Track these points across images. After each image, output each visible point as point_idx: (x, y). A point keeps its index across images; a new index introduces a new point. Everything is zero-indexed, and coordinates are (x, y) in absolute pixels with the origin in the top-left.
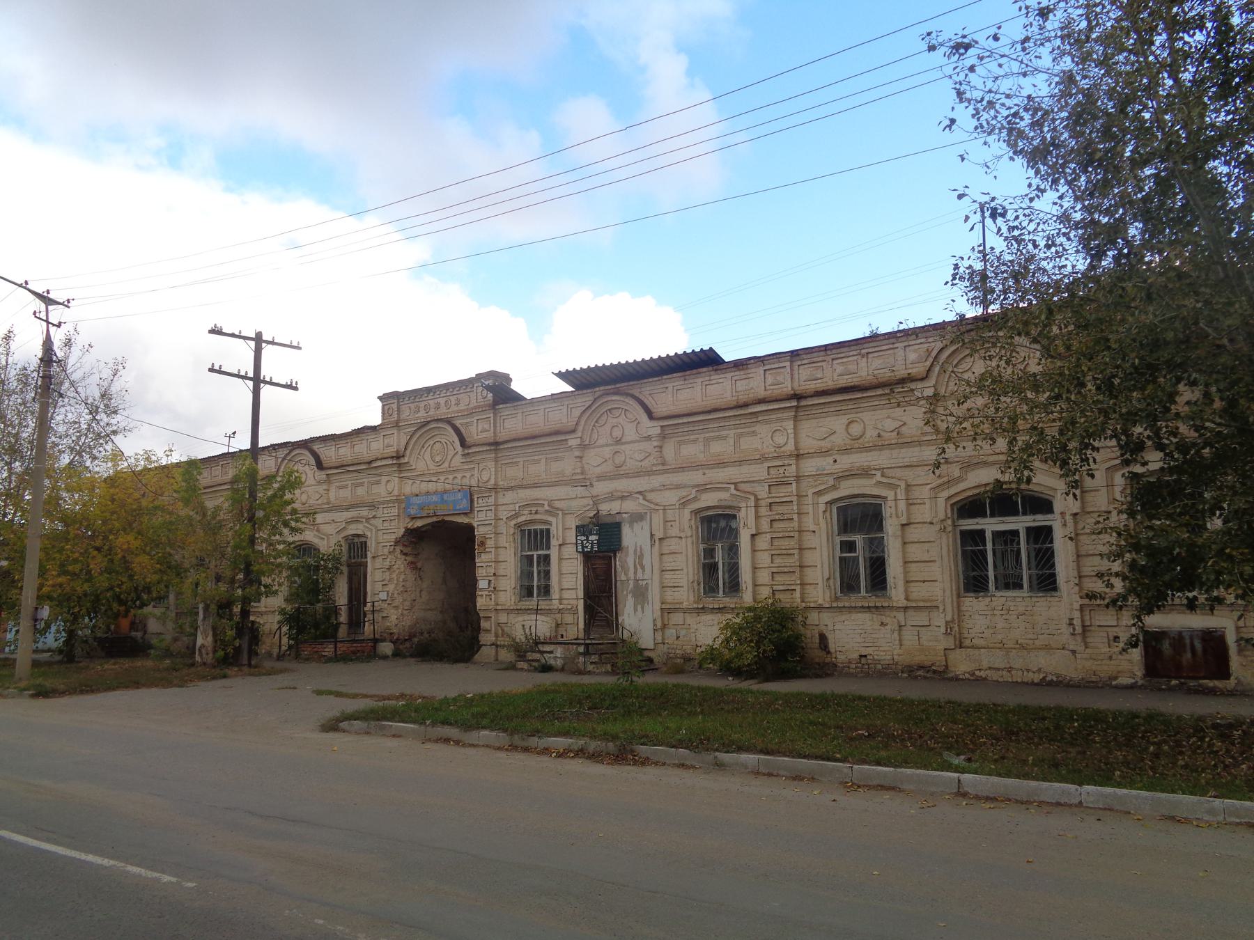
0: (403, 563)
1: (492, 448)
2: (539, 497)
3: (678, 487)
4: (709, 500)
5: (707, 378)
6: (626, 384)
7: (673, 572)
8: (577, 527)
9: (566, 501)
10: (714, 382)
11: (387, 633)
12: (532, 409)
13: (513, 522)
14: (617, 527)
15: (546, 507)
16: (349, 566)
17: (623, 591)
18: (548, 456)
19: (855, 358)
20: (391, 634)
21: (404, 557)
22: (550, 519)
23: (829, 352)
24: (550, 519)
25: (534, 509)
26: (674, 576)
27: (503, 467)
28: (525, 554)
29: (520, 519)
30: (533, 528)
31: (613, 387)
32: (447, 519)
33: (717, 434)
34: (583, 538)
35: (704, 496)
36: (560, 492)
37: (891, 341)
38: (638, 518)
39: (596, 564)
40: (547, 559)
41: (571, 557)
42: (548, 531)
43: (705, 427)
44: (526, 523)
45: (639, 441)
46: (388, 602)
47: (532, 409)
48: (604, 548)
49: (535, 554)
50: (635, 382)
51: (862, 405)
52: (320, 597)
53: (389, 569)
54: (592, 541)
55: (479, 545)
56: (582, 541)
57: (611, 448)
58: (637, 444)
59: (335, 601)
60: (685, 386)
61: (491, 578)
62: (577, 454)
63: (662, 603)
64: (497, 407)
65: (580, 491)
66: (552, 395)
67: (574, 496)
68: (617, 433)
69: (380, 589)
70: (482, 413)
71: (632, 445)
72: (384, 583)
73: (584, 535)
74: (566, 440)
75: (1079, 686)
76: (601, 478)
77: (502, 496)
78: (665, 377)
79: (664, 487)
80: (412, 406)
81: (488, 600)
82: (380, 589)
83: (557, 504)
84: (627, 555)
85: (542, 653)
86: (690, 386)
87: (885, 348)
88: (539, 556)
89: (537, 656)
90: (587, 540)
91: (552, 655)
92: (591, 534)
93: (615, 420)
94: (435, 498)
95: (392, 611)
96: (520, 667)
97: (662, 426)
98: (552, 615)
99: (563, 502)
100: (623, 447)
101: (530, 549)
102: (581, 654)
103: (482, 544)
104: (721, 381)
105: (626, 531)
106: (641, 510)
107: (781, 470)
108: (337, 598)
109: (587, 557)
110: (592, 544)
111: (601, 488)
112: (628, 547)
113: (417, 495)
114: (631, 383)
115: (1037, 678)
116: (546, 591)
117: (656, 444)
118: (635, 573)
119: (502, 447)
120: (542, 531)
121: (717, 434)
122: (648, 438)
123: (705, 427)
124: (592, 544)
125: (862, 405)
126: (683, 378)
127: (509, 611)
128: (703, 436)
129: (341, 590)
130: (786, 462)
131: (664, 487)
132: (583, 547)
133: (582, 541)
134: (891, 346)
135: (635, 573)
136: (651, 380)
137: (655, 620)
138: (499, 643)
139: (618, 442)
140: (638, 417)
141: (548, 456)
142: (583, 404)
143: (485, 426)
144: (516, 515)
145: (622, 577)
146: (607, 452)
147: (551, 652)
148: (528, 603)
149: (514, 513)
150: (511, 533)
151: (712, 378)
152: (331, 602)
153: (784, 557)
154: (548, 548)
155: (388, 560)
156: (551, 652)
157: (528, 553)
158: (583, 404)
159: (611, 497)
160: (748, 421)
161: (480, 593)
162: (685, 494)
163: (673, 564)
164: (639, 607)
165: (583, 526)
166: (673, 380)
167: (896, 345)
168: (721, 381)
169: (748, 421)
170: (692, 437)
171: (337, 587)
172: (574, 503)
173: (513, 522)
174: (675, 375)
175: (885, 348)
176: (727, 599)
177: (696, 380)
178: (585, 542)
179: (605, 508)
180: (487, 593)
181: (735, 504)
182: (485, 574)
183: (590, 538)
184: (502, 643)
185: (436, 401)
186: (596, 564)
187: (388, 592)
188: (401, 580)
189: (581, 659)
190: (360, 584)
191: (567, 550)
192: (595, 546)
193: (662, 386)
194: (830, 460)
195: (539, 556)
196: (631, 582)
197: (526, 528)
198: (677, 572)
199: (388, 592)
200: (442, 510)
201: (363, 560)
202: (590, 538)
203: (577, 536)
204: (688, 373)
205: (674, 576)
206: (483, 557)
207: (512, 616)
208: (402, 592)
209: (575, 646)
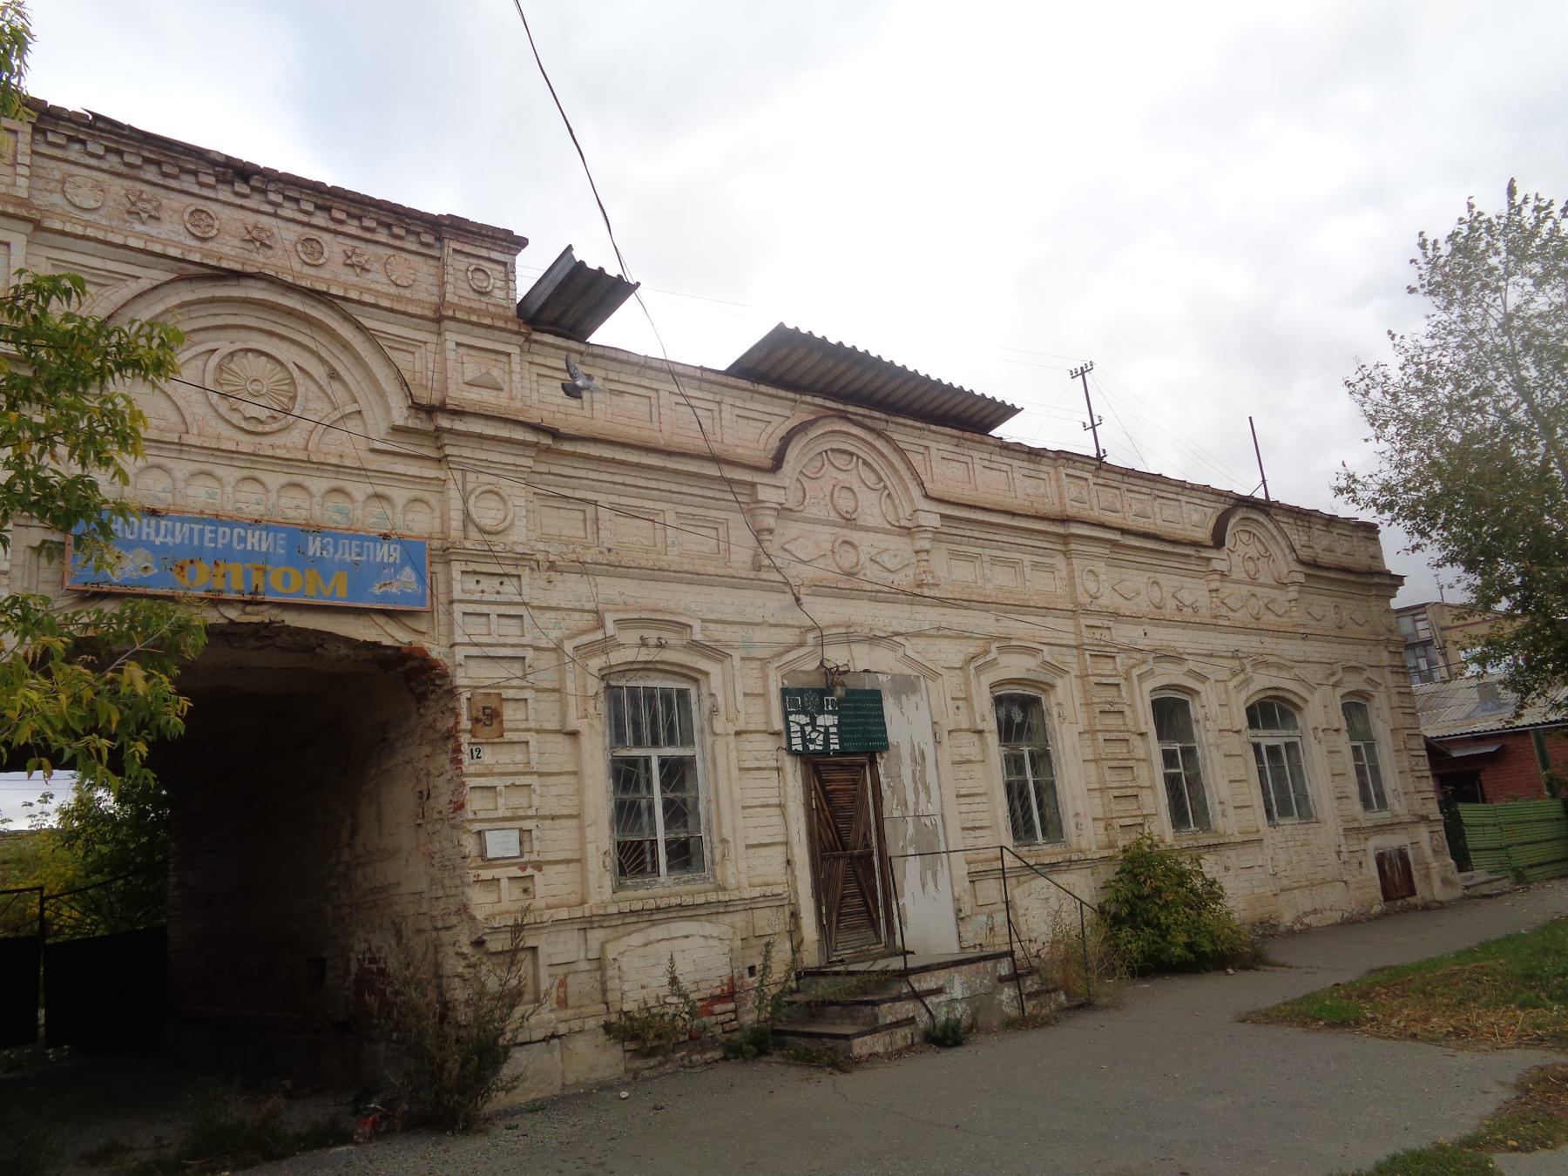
1: (546, 441)
2: (662, 605)
3: (961, 635)
4: (1015, 666)
5: (987, 456)
6: (866, 412)
7: (968, 800)
8: (785, 692)
9: (735, 628)
10: (994, 465)
12: (635, 380)
13: (595, 663)
14: (875, 697)
15: (698, 636)
17: (897, 844)
18: (681, 509)
19: (1146, 497)
22: (703, 664)
23: (1126, 479)
24: (703, 664)
25: (652, 636)
26: (975, 808)
27: (537, 503)
28: (624, 753)
29: (617, 657)
30: (641, 684)
31: (841, 407)
32: (293, 620)
33: (1006, 554)
34: (804, 719)
35: (1005, 660)
36: (725, 602)
37: (1179, 490)
38: (906, 686)
39: (830, 781)
40: (677, 772)
41: (763, 764)
42: (682, 694)
43: (997, 537)
44: (631, 668)
45: (886, 532)
47: (635, 380)
48: (851, 746)
49: (654, 755)
50: (883, 416)
51: (1165, 563)
54: (827, 728)
55: (476, 720)
56: (802, 726)
57: (836, 530)
58: (881, 536)
60: (955, 457)
61: (527, 825)
62: (769, 521)
63: (968, 863)
64: (536, 336)
65: (771, 605)
66: (702, 369)
67: (759, 620)
68: (845, 502)
70: (483, 332)
71: (872, 535)
73: (804, 712)
74: (753, 485)
75: (1359, 921)
76: (822, 589)
77: (543, 583)
78: (933, 427)
79: (939, 633)
80: (117, 186)
81: (517, 893)
83: (717, 632)
84: (899, 764)
85: (918, 996)
86: (962, 458)
87: (1170, 496)
88: (664, 762)
89: (907, 1009)
90: (813, 723)
91: (943, 998)
92: (821, 712)
93: (841, 476)
94: (256, 541)
96: (865, 1051)
97: (943, 516)
98: (727, 918)
99: (728, 627)
100: (855, 536)
101: (638, 742)
102: (1002, 979)
103: (489, 716)
104: (1004, 468)
105: (889, 708)
106: (907, 671)
107: (1098, 633)
109: (814, 764)
110: (827, 734)
111: (825, 611)
112: (898, 745)
113: (153, 513)
114: (876, 414)
115: (1337, 917)
116: (684, 855)
117: (927, 545)
118: (917, 803)
119: (568, 447)
120: (666, 696)
121: (1006, 554)
122: (908, 532)
123: (997, 537)
124: (827, 734)
125: (1165, 563)
126: (954, 441)
127: (587, 924)
128: (987, 551)
130: (1106, 623)
131: (939, 633)
132: (806, 740)
133: (802, 726)
134: (1175, 496)
135: (917, 803)
136: (910, 422)
137: (956, 900)
138: (562, 1029)
139: (849, 521)
140: (889, 484)
141: (681, 509)
142: (766, 418)
143: (495, 373)
144: (606, 645)
145: (891, 807)
146: (825, 535)
147: (938, 991)
148: (641, 893)
149: (599, 635)
150: (591, 692)
151: (994, 458)
153: (1120, 771)
154: (688, 741)
156: (938, 991)
157: (636, 752)
158: (766, 418)
159: (849, 638)
160: (1050, 546)
161: (486, 874)
162: (972, 650)
163: (968, 783)
164: (929, 874)
165: (801, 692)
166: (939, 437)
167: (1180, 497)
168: (1004, 468)
169: (1050, 546)
170: (972, 550)
172: (759, 635)
173: (595, 663)
174: (948, 430)
175: (1170, 496)
176: (1048, 846)
177: (972, 453)
178: (808, 729)
179: (837, 656)
180: (517, 872)
181: (1048, 679)
182: (501, 813)
183: (821, 720)
184: (576, 1025)
185: (251, 218)
186: (830, 781)
189: (1008, 992)
191: (749, 747)
192: (834, 740)
193: (919, 441)
194: (1140, 630)
195: (664, 762)
196: (911, 830)
197: (622, 683)
198: (977, 799)
200: (278, 586)
202: (821, 720)
203: (786, 715)
204: (968, 435)
205: (975, 808)
206: (488, 755)
207: (596, 936)
209: (989, 964)
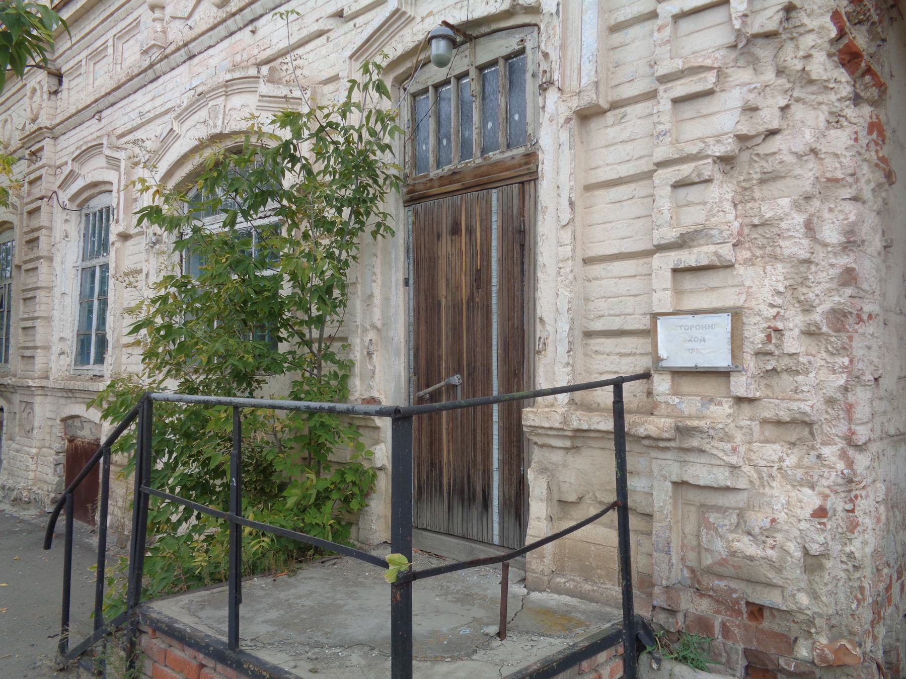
0: (836, 120)
11: (723, 602)
16: (413, 199)
20: (757, 611)
21: (842, 75)
46: (740, 385)
52: (283, 347)
53: (726, 161)
59: (348, 366)
69: (663, 300)
72: (689, 258)
82: (663, 300)
95: (773, 451)
108: (357, 354)
129: (377, 316)
152: (328, 368)
155: (733, 98)
171: (357, 303)
187: (736, 315)
188: (831, 234)
190: (480, 278)
199: (736, 315)
201: (495, 156)
208: (838, 317)
